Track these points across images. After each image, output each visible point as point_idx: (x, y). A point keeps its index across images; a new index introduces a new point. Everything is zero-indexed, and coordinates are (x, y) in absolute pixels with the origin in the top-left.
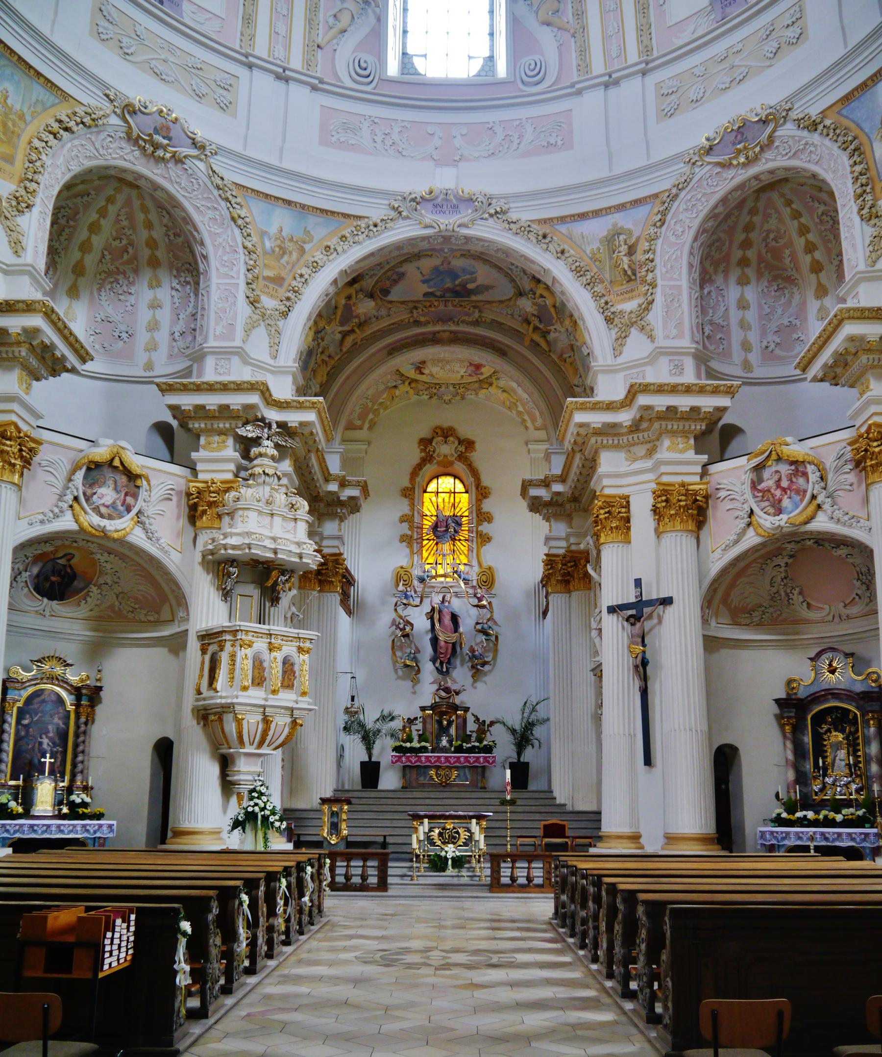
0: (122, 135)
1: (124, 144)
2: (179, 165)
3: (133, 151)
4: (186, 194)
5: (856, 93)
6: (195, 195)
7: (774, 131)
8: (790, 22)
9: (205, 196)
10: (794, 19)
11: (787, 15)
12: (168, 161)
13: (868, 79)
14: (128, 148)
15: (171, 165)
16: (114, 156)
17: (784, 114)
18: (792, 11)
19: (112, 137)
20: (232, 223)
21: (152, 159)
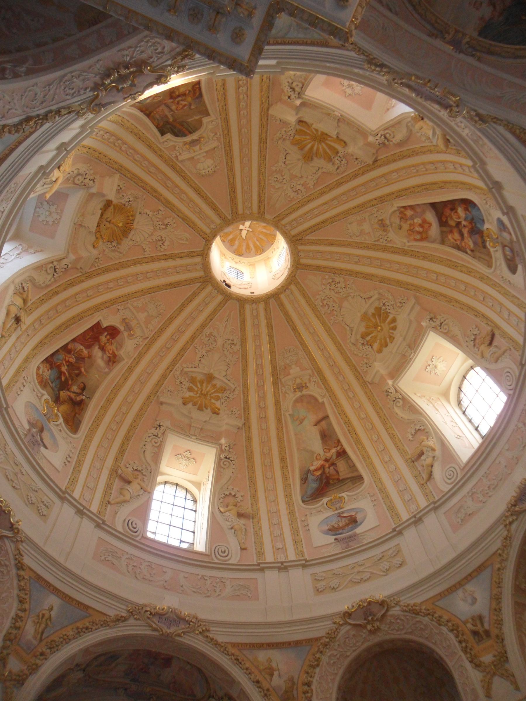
0: (152, 60)
1: (144, 56)
2: (92, 85)
3: (132, 58)
4: (66, 78)
5: (43, 582)
6: (61, 86)
7: (7, 537)
8: (45, 503)
9: (56, 97)
10: (47, 504)
11: (46, 497)
12: (103, 79)
13: (53, 586)
14: (138, 56)
15: (98, 79)
16: (142, 43)
17: (19, 539)
18: (49, 501)
19: (159, 53)
20: (24, 117)
21: (112, 66)
